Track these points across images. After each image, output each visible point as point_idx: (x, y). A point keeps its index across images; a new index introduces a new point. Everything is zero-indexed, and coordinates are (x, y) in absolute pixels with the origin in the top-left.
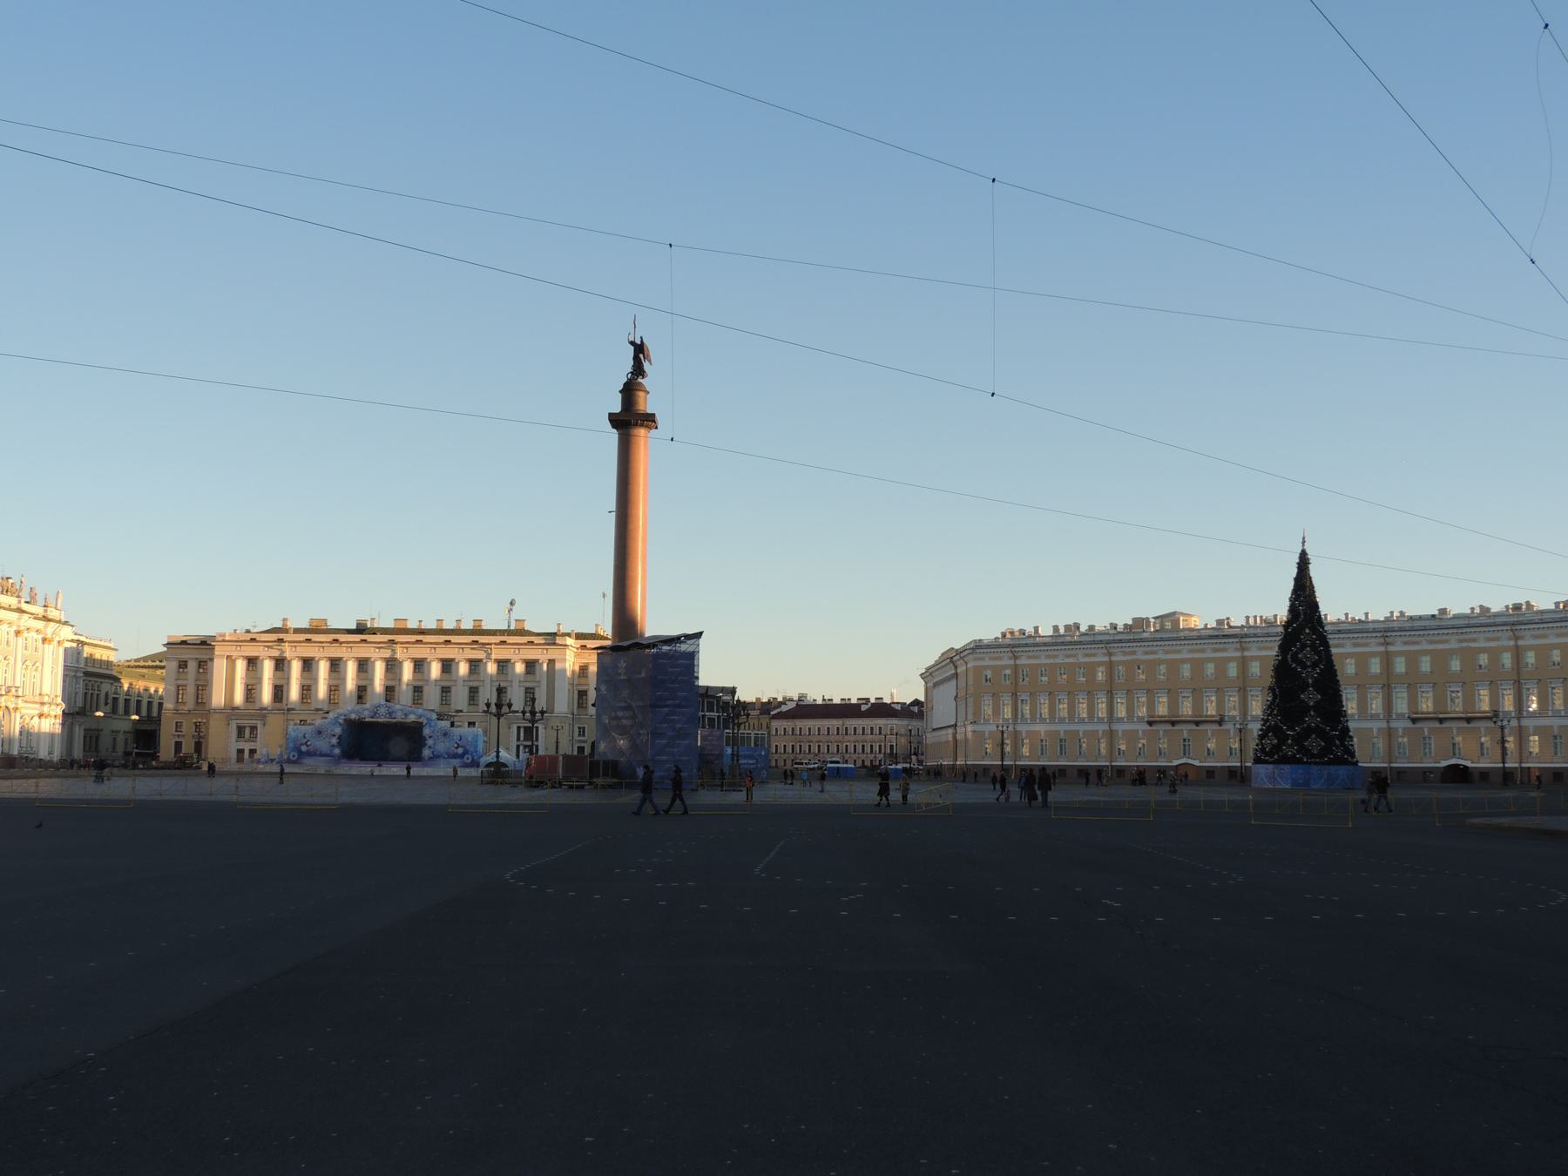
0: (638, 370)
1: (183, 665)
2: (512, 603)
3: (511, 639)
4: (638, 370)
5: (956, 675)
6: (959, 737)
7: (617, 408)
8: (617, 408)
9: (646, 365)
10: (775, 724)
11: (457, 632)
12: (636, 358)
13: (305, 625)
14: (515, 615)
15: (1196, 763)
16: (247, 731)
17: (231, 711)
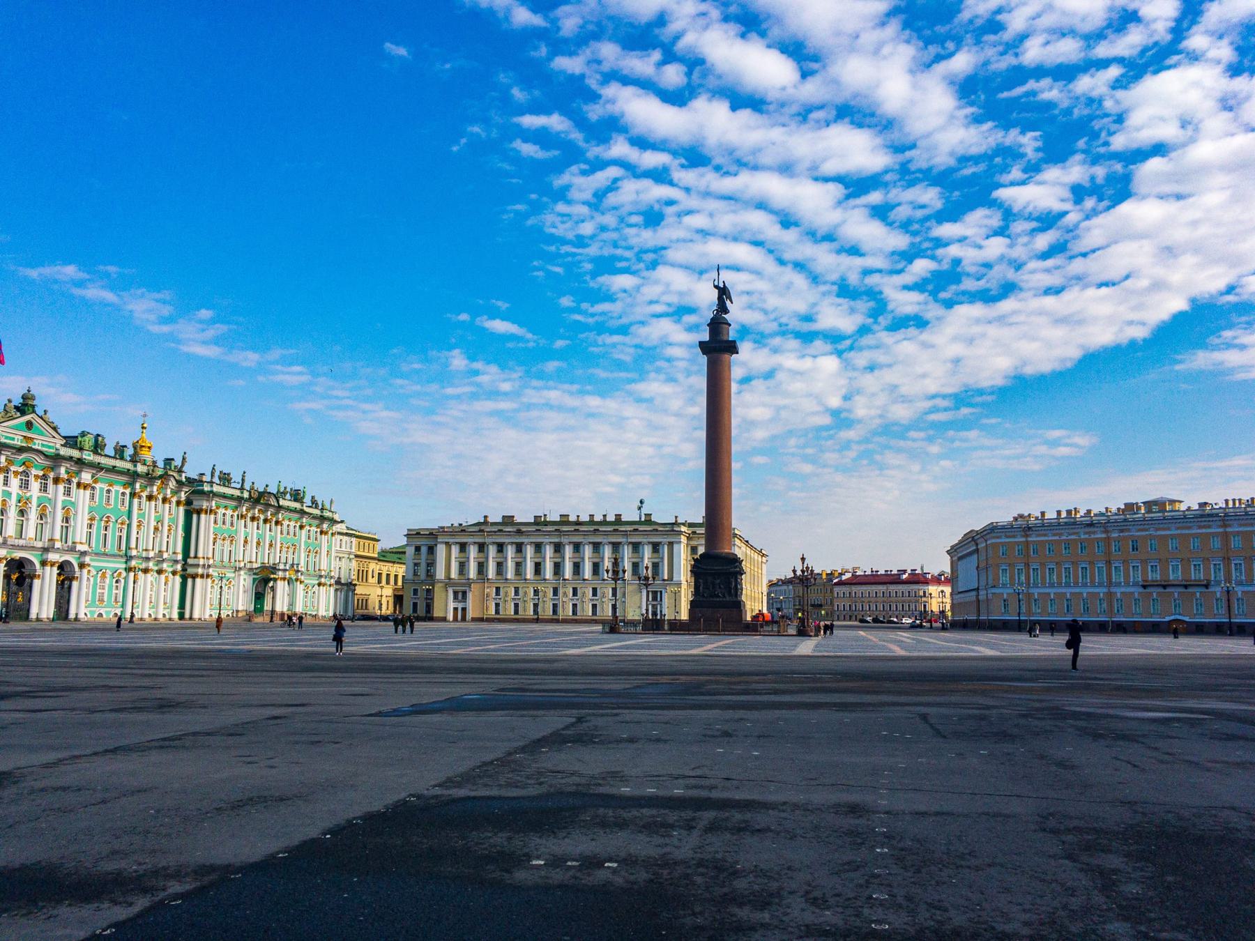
0: (722, 308)
1: (418, 549)
2: (641, 502)
3: (641, 528)
4: (722, 308)
5: (977, 551)
6: (981, 598)
7: (706, 337)
8: (706, 337)
9: (728, 303)
10: (836, 589)
11: (604, 522)
12: (720, 298)
13: (499, 520)
14: (644, 511)
15: (1187, 619)
16: (460, 596)
17: (448, 582)
